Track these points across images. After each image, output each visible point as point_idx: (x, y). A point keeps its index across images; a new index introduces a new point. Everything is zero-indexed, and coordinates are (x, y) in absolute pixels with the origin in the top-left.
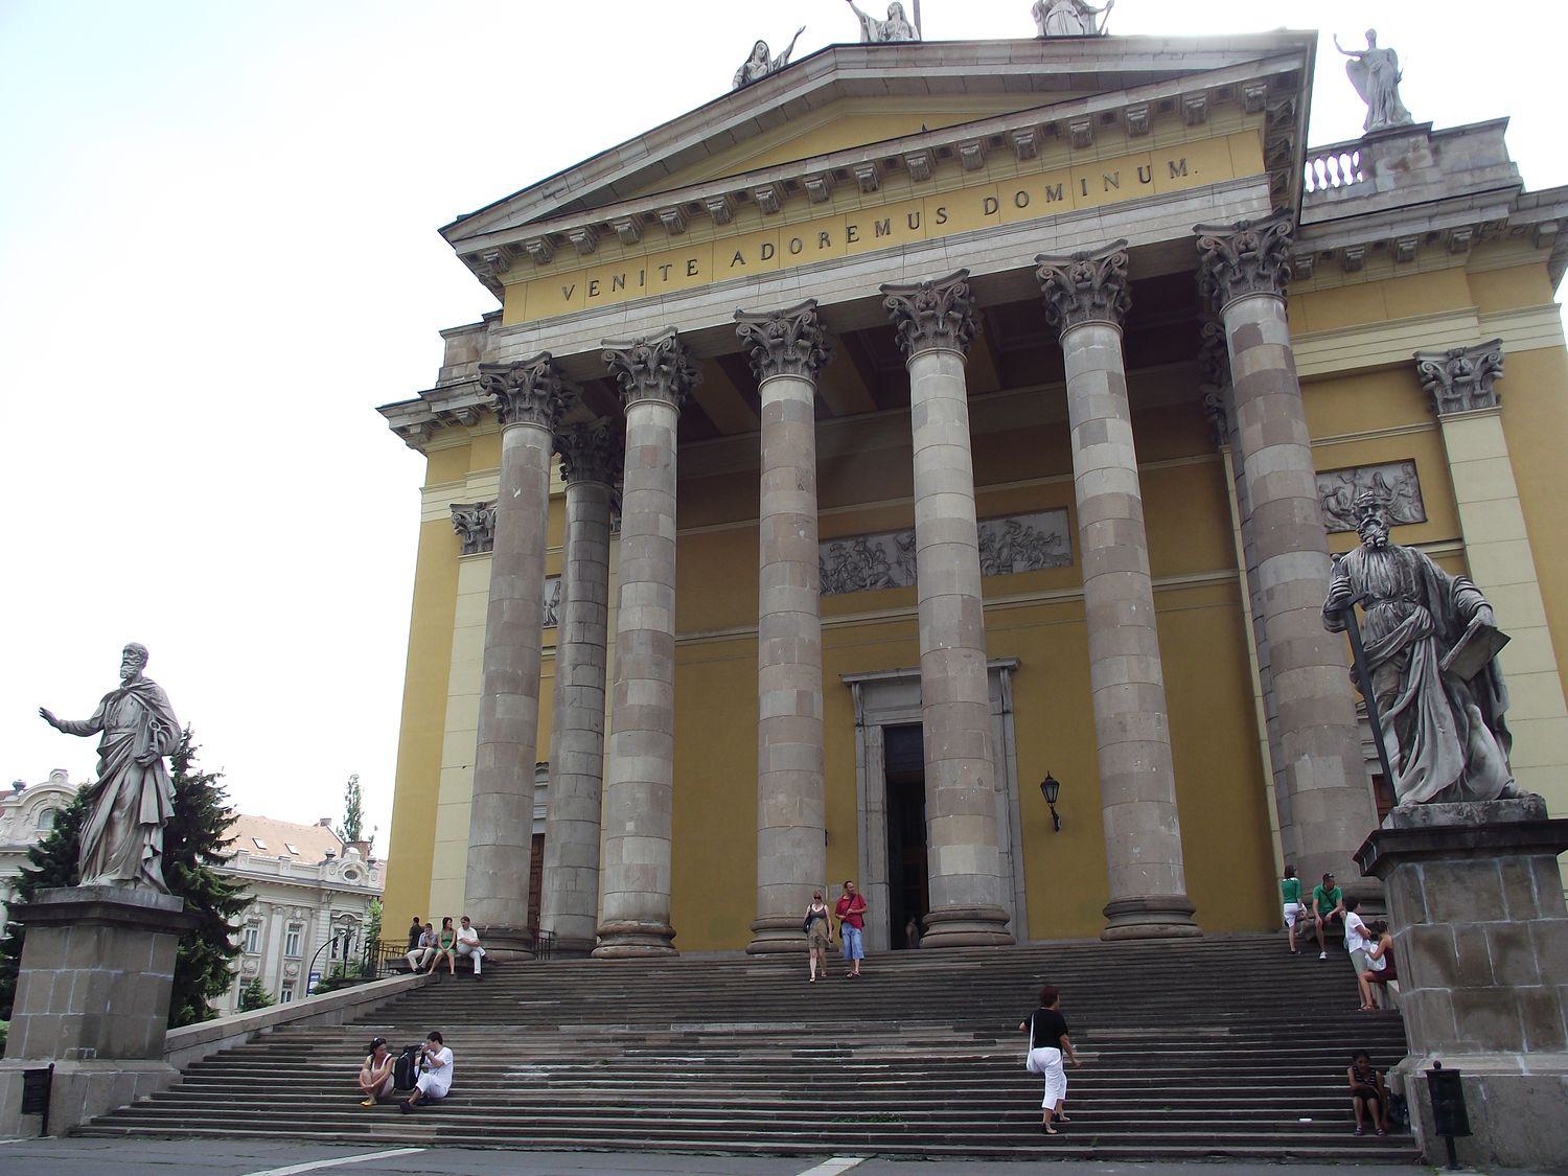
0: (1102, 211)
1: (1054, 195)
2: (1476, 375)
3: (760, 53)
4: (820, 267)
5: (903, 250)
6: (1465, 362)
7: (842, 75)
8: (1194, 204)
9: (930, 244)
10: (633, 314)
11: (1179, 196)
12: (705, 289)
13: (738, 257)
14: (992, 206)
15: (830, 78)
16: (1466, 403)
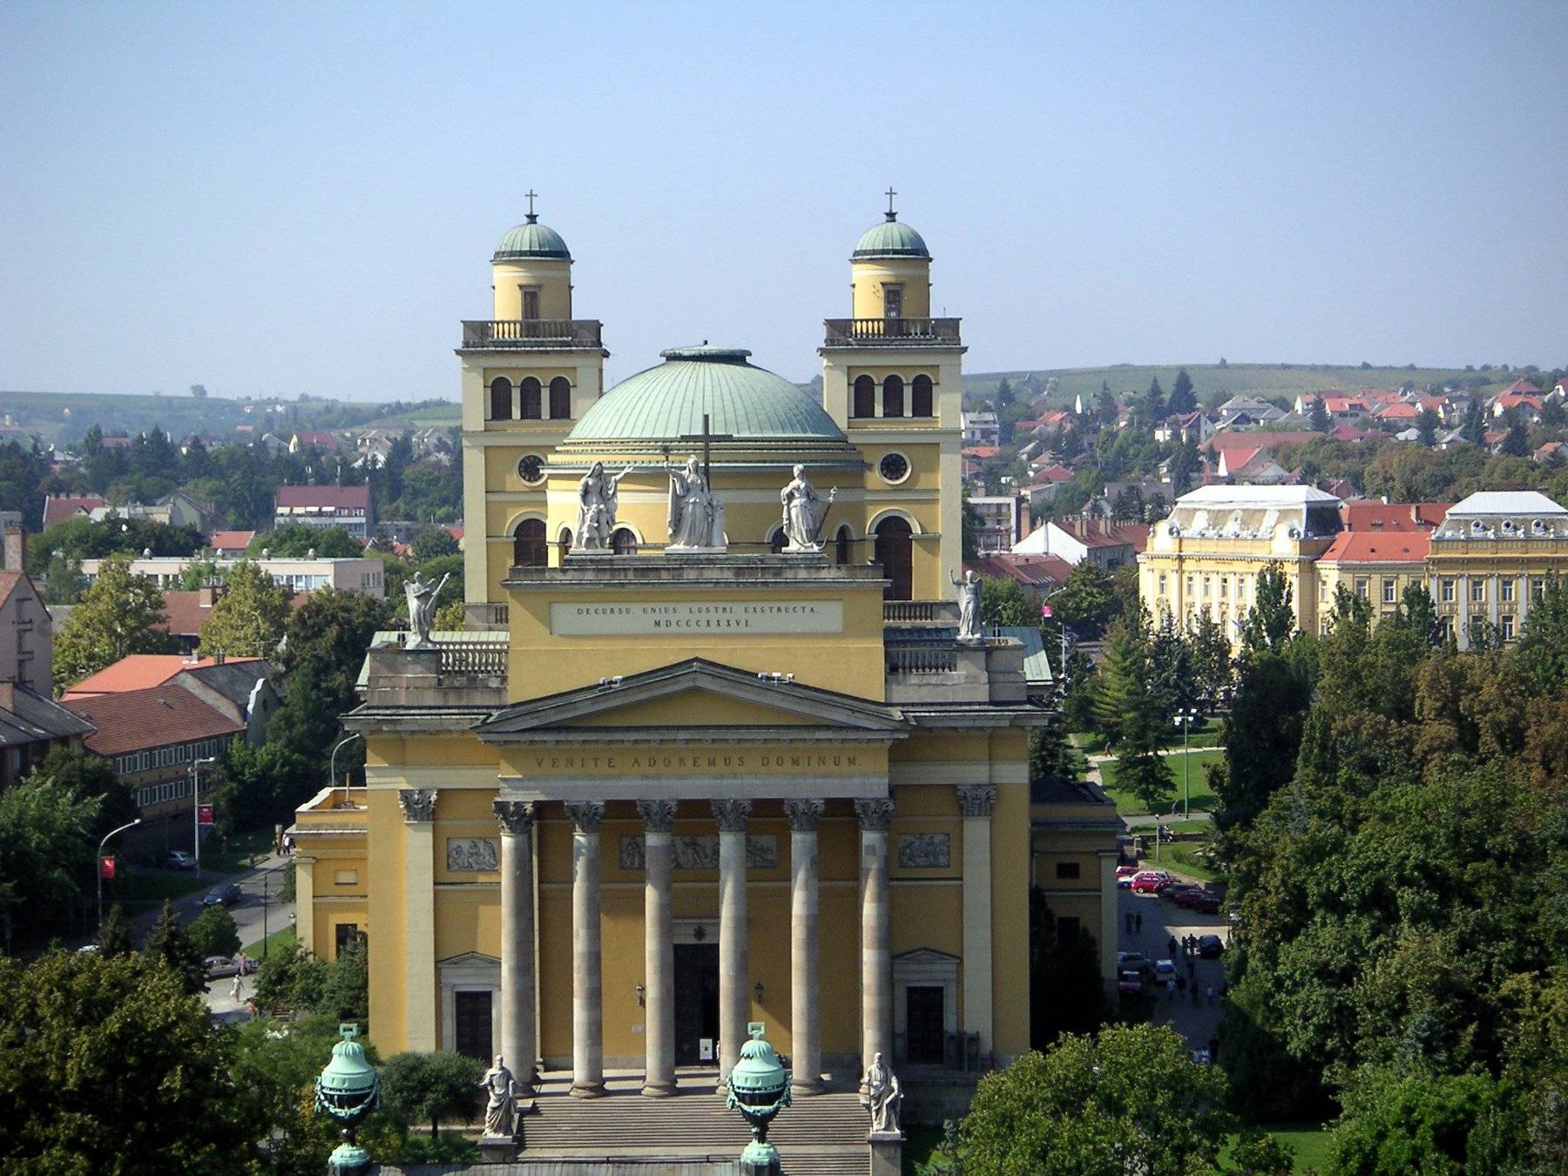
0: (815, 776)
1: (795, 762)
2: (983, 799)
3: (596, 473)
4: (679, 777)
5: (722, 777)
6: (982, 794)
7: (699, 684)
8: (856, 781)
9: (735, 776)
10: (579, 783)
11: (851, 776)
12: (619, 777)
13: (636, 761)
14: (765, 761)
15: (691, 684)
16: (976, 812)
